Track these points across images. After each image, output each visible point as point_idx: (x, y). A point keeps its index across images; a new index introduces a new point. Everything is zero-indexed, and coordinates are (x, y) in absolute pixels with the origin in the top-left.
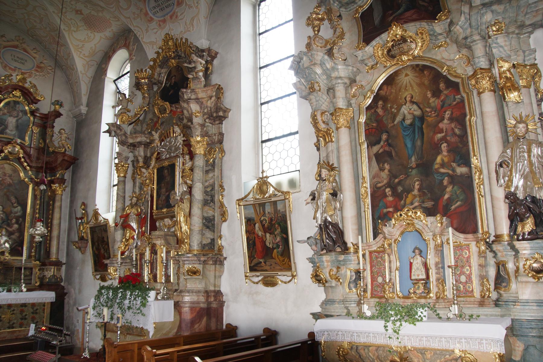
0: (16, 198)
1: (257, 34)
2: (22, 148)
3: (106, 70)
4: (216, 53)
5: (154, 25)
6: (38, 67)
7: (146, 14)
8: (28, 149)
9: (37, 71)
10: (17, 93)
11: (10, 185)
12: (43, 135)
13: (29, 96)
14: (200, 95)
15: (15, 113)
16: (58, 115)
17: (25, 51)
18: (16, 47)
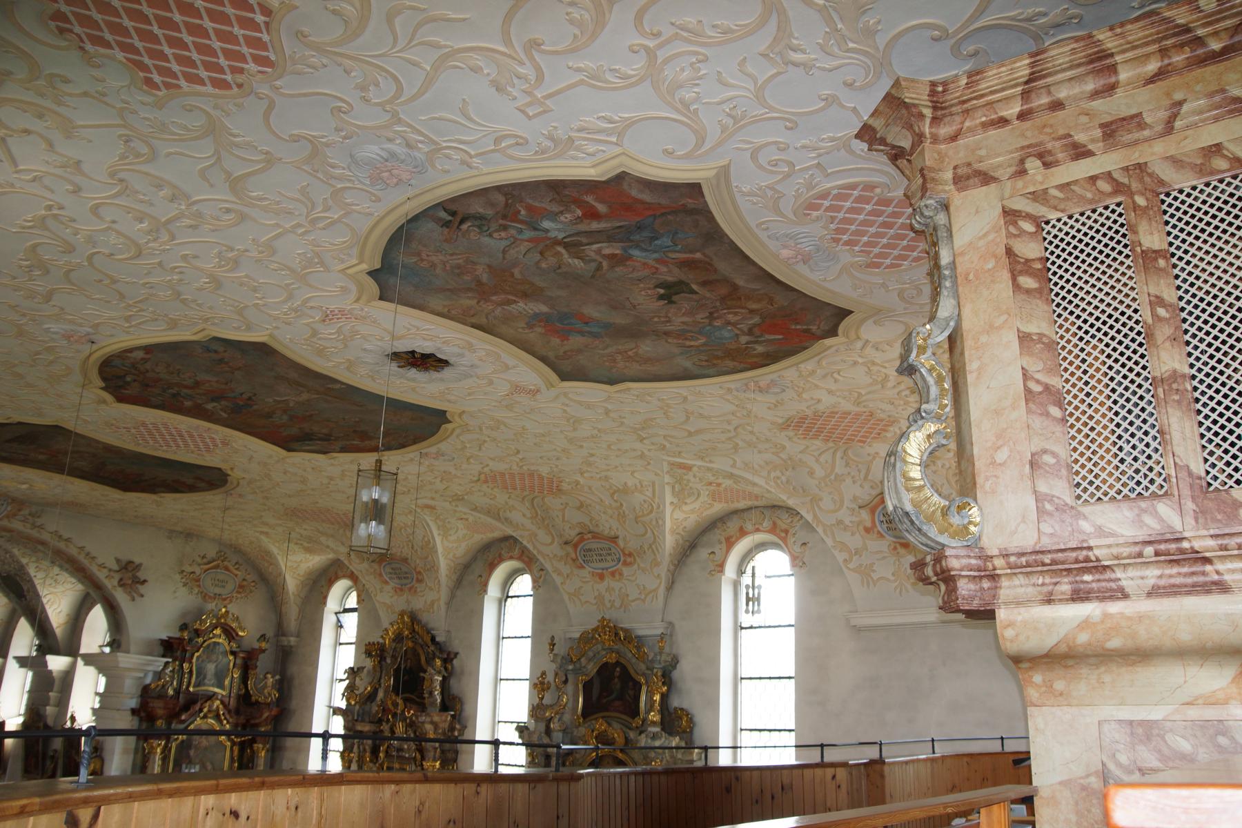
0: (212, 764)
1: (499, 638)
2: (222, 702)
3: (325, 597)
4: (456, 654)
5: (388, 588)
6: (241, 586)
7: (381, 575)
8: (226, 700)
9: (238, 592)
10: (218, 631)
11: (206, 748)
12: (244, 679)
13: (230, 633)
14: (436, 719)
15: (214, 657)
16: (263, 651)
17: (227, 569)
18: (217, 567)
